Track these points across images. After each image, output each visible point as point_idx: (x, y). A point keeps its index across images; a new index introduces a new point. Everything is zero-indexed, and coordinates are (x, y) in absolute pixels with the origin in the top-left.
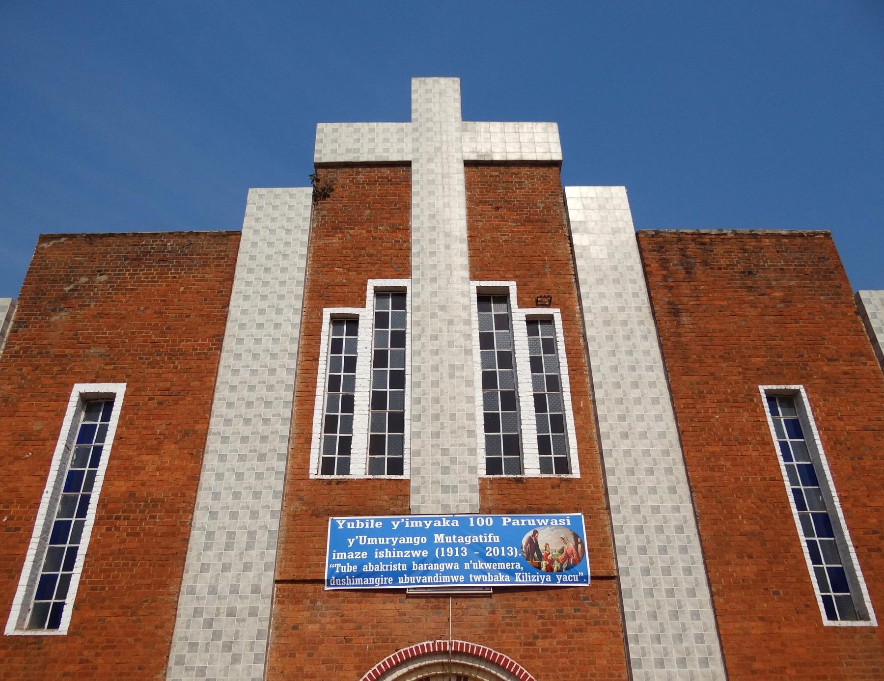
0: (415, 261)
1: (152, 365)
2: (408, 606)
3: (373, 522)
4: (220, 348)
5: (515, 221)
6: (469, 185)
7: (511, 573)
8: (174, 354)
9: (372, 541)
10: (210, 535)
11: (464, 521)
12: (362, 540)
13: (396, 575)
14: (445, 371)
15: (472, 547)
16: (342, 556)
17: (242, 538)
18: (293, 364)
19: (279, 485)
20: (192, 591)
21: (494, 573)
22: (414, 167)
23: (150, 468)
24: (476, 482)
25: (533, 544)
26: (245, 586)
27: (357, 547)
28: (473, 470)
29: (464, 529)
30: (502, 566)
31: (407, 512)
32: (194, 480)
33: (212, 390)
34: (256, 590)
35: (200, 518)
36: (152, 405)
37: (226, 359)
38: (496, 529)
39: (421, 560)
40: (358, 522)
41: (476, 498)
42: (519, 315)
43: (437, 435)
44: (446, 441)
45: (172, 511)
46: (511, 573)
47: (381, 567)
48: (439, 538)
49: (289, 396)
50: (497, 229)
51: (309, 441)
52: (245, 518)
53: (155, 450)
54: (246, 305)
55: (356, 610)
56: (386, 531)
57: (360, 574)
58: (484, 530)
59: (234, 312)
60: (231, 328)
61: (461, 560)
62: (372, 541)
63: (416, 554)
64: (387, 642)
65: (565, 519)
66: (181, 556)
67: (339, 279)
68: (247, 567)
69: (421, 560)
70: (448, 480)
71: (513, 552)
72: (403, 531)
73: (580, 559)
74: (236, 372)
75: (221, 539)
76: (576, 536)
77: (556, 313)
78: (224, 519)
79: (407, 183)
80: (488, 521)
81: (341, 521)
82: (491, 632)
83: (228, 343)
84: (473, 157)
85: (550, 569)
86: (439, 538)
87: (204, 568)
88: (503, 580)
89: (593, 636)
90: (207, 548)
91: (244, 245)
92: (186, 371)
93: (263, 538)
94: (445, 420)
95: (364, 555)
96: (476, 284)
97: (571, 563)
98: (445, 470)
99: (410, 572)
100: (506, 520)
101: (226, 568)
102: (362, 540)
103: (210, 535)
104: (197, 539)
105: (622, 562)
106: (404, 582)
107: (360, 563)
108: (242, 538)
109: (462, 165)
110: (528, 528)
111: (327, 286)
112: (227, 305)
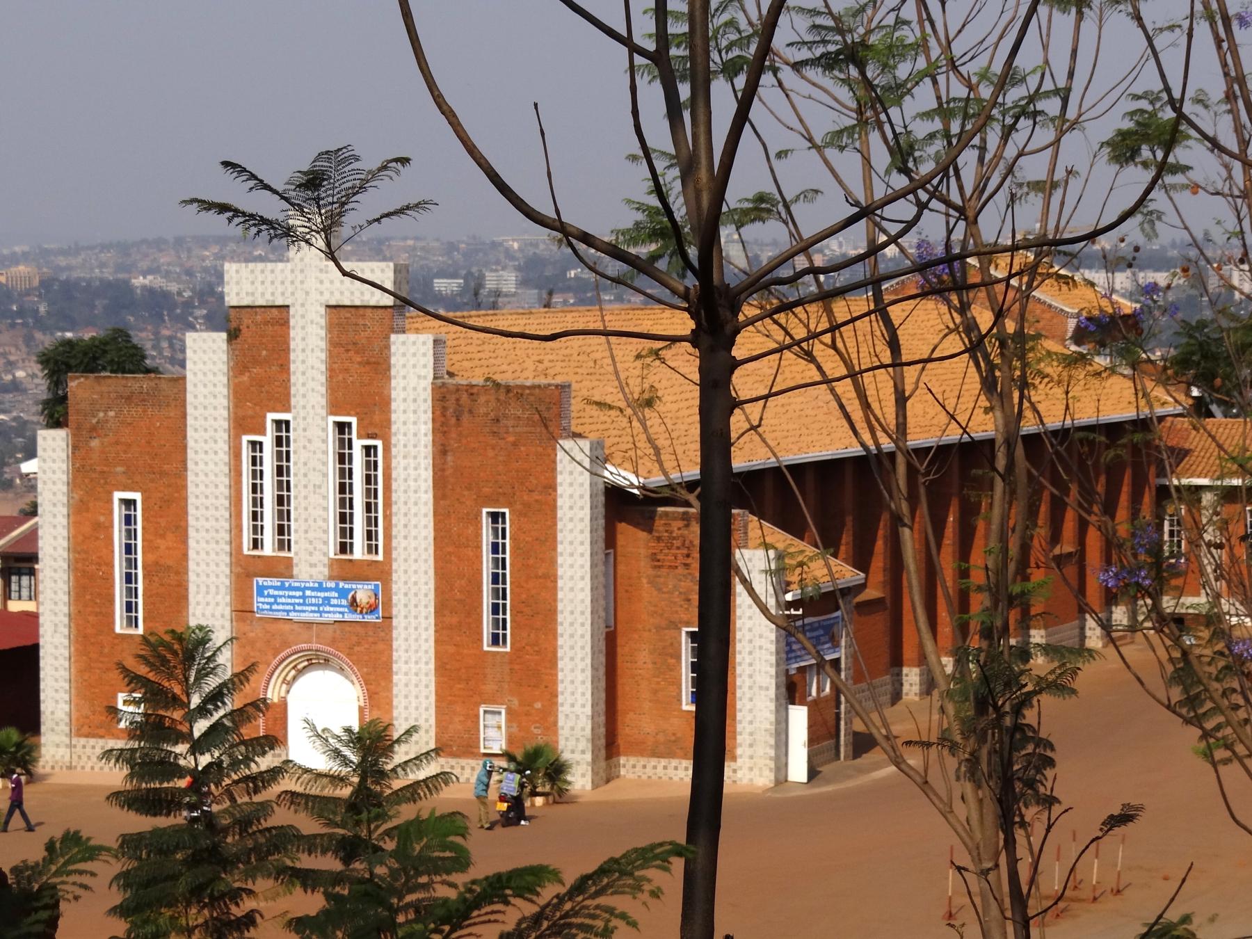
0: (293, 401)
1: (152, 481)
2: (295, 627)
3: (275, 582)
4: (185, 469)
5: (359, 363)
6: (330, 327)
7: (343, 613)
8: (162, 474)
9: (276, 593)
10: (198, 586)
11: (320, 584)
12: (272, 592)
13: (288, 611)
14: (311, 488)
15: (325, 598)
16: (262, 600)
17: (213, 589)
18: (227, 481)
19: (227, 560)
20: (194, 615)
21: (334, 613)
22: (292, 311)
23: (163, 547)
24: (326, 561)
25: (354, 599)
26: (218, 614)
27: (269, 596)
28: (325, 554)
29: (321, 588)
30: (338, 609)
31: (291, 577)
32: (185, 556)
33: (186, 499)
34: (223, 616)
35: (192, 577)
36: (156, 508)
37: (191, 477)
38: (336, 589)
39: (299, 604)
40: (269, 582)
41: (326, 571)
42: (358, 444)
43: (306, 532)
44: (311, 535)
45: (177, 573)
46: (343, 613)
47: (281, 607)
48: (308, 593)
49: (227, 503)
50: (347, 370)
51: (241, 530)
52: (213, 578)
53: (163, 536)
54: (196, 435)
55: (272, 627)
56: (282, 588)
57: (271, 610)
58: (327, 590)
59: (191, 443)
60: (190, 454)
61: (318, 605)
62: (276, 593)
63: (297, 601)
64: (286, 644)
65: (370, 586)
66: (185, 597)
67: (250, 412)
68: (217, 604)
69: (299, 604)
70: (314, 560)
71: (344, 602)
72: (291, 588)
73: (377, 607)
74: (197, 485)
75: (203, 589)
76: (376, 595)
77: (378, 443)
78: (203, 578)
79: (285, 323)
80: (332, 584)
81: (260, 580)
82: (333, 642)
83: (190, 465)
84: (333, 303)
85: (361, 612)
86: (308, 593)
87: (198, 603)
88: (338, 617)
89: (381, 646)
90: (198, 593)
91: (189, 387)
92: (170, 486)
93: (223, 590)
94: (311, 522)
95: (272, 600)
96: (332, 419)
97: (372, 609)
98: (311, 554)
99: (295, 611)
100: (341, 584)
101: (208, 604)
102: (272, 592)
103: (198, 586)
104: (192, 589)
105: (395, 611)
106: (292, 615)
107: (271, 604)
108: (213, 589)
109: (322, 310)
110: (352, 589)
111: (244, 418)
112: (185, 437)
